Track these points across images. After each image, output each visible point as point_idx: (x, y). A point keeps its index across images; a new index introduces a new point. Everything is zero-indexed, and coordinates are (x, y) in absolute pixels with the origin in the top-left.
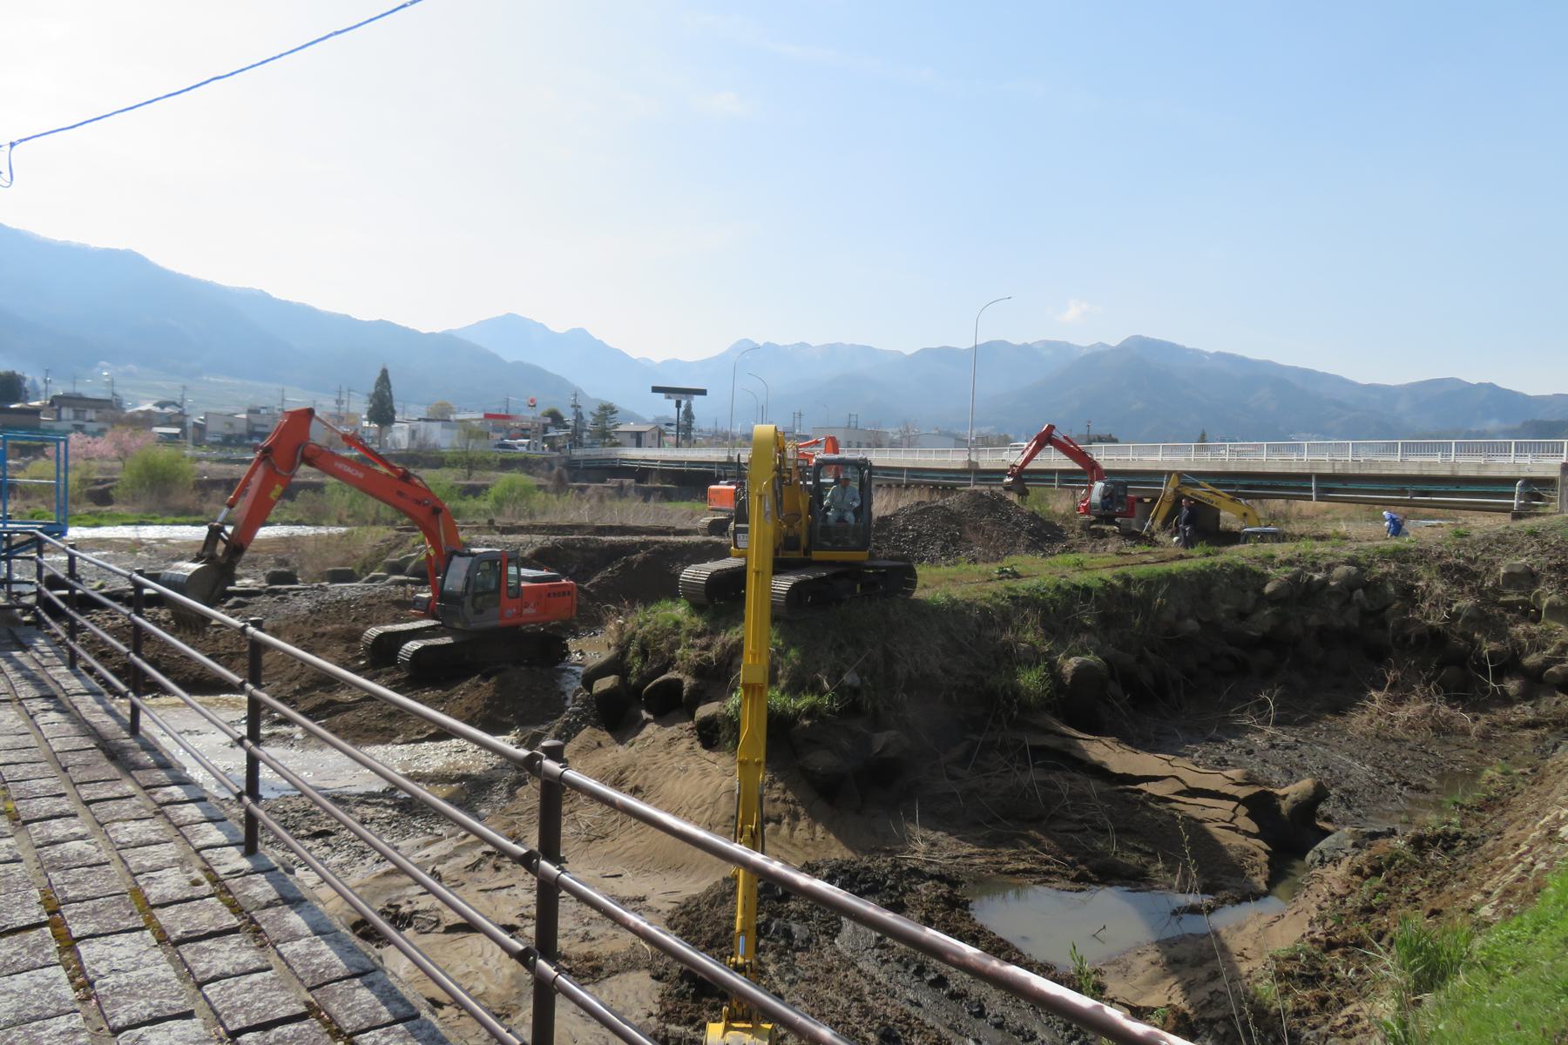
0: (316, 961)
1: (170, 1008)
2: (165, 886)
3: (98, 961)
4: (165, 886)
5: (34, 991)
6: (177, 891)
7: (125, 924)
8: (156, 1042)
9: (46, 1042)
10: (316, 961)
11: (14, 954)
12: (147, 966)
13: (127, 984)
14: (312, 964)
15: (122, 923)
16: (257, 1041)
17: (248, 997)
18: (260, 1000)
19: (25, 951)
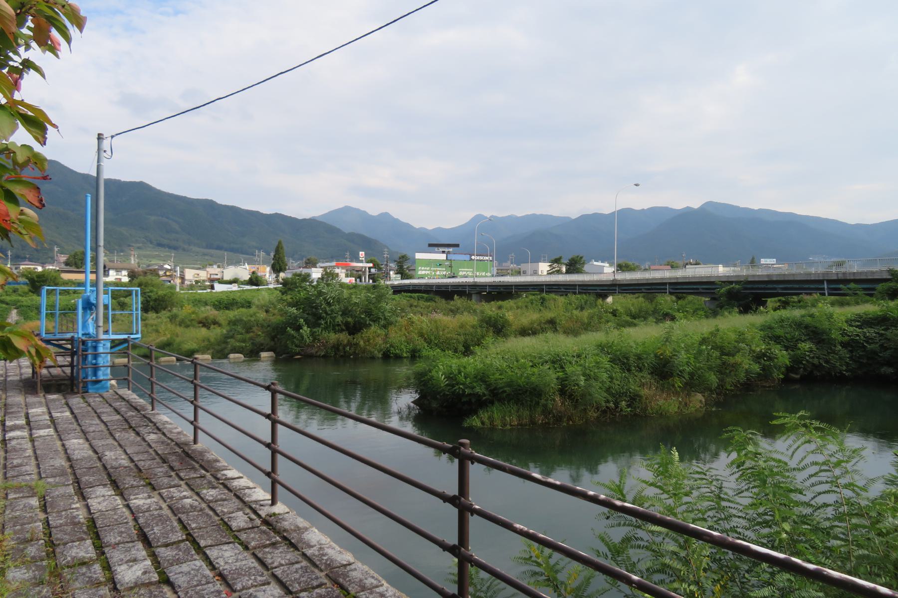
0: (325, 558)
1: (260, 581)
2: (238, 521)
3: (217, 558)
4: (238, 521)
5: (192, 572)
6: (244, 524)
7: (224, 540)
8: (364, 596)
9: (207, 596)
10: (325, 558)
11: (176, 554)
12: (241, 560)
13: (236, 569)
14: (323, 559)
15: (223, 539)
16: (308, 597)
17: (297, 576)
18: (303, 577)
19: (181, 553)
